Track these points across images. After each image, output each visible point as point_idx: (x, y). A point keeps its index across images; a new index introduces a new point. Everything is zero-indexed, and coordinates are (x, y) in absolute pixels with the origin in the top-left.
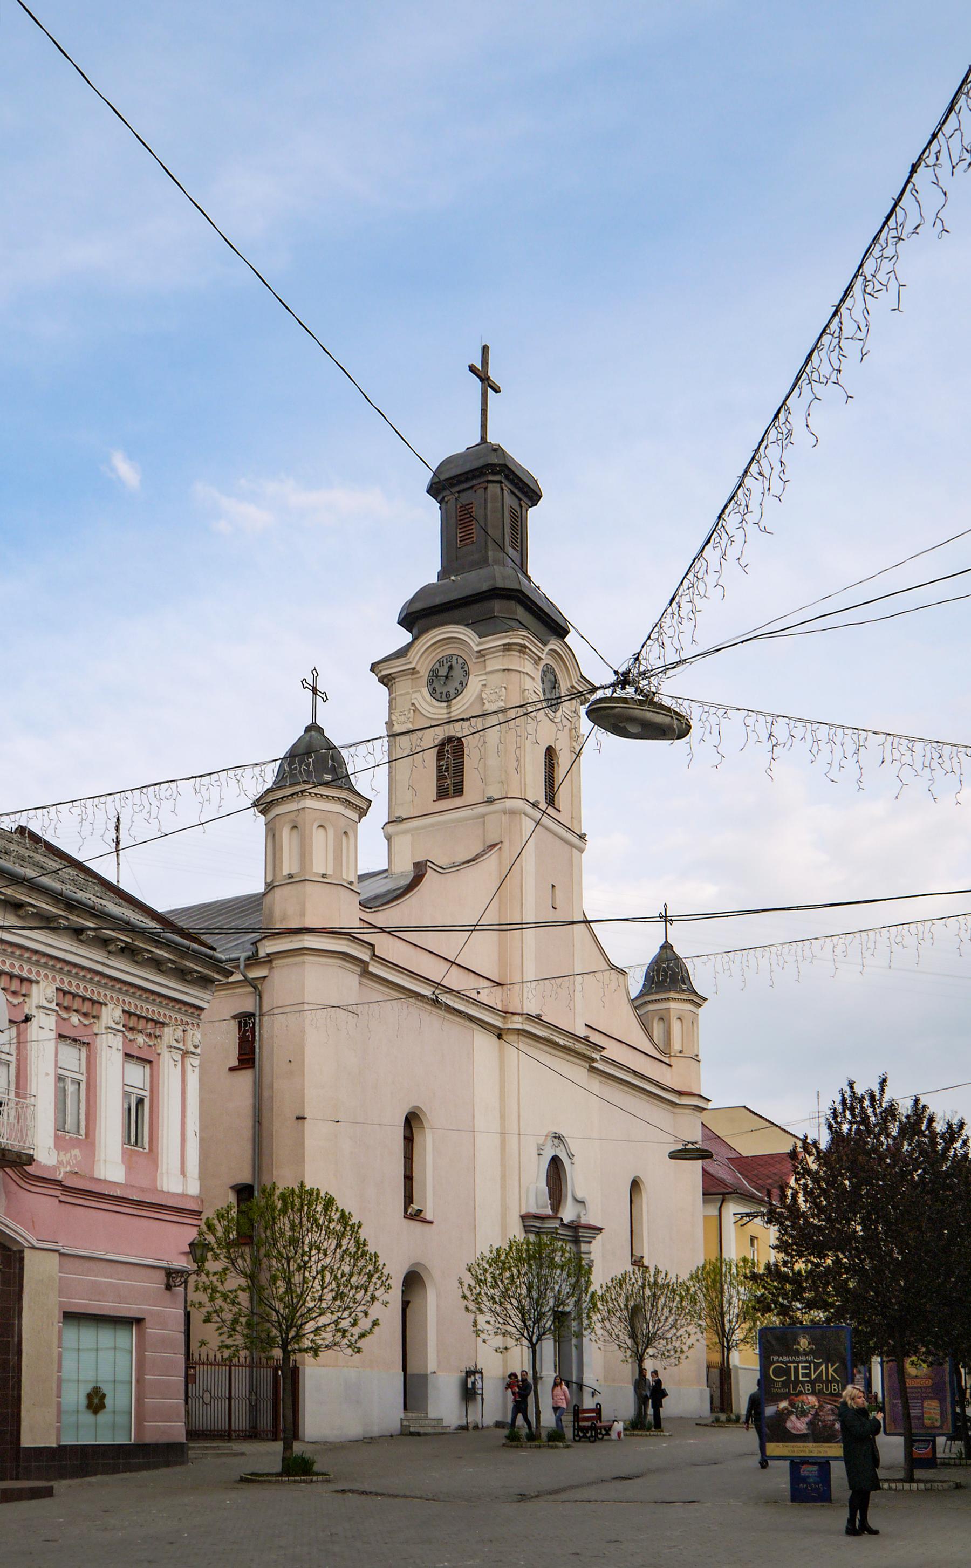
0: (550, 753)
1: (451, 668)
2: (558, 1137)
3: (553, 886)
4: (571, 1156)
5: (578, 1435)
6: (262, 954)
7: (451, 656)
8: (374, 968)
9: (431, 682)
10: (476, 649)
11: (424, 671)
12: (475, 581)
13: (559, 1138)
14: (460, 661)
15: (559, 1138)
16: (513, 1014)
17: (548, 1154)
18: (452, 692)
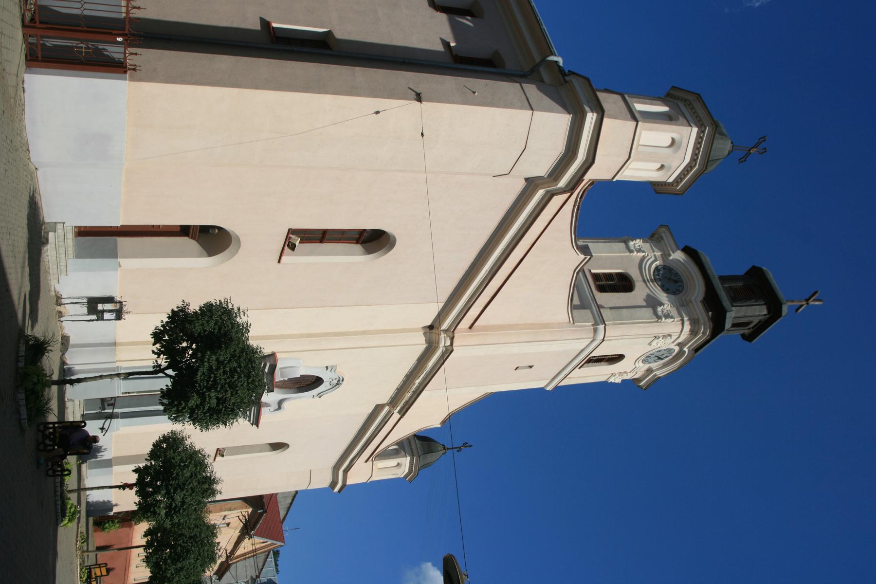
0: (620, 358)
1: (676, 282)
3: (531, 367)
4: (320, 395)
6: (567, 78)
7: (682, 282)
8: (540, 193)
10: (693, 298)
13: (337, 384)
14: (681, 288)
15: (337, 384)
16: (452, 339)
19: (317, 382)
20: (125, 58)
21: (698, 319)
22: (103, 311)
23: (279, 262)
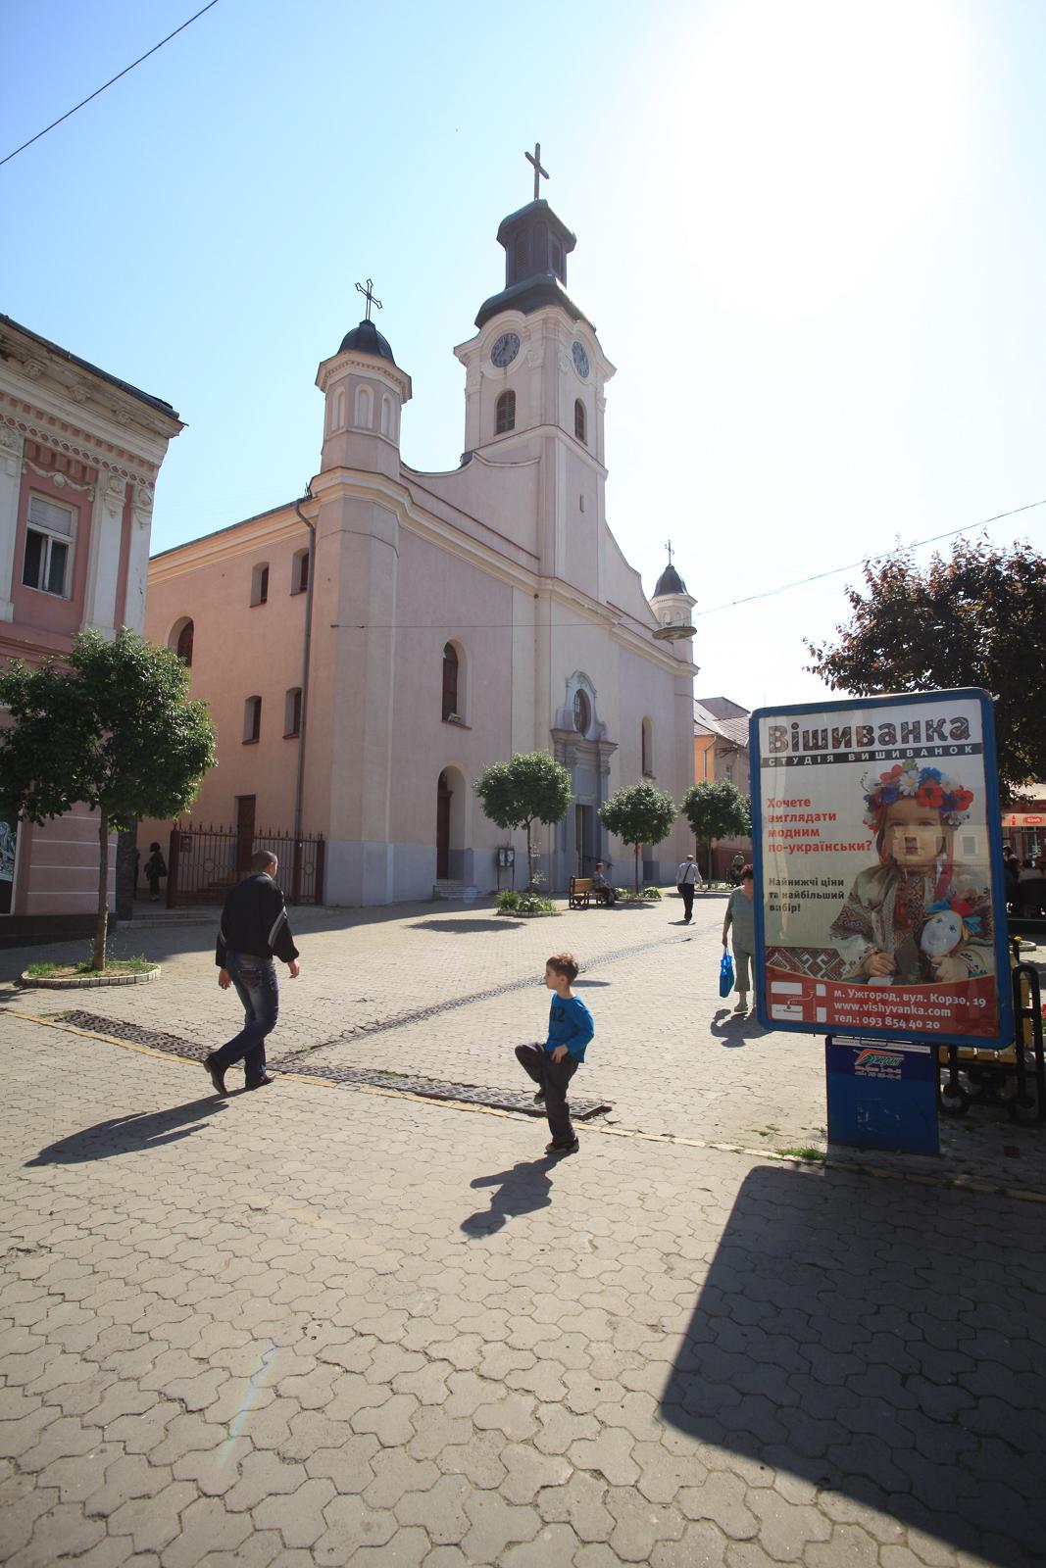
1: (506, 343)
2: (583, 677)
4: (594, 692)
5: (573, 903)
6: (314, 496)
7: (507, 335)
9: (493, 355)
10: (523, 325)
11: (488, 351)
12: (522, 285)
17: (575, 687)
18: (508, 359)
19: (581, 694)
20: (314, 842)
21: (543, 320)
22: (506, 861)
23: (469, 729)
